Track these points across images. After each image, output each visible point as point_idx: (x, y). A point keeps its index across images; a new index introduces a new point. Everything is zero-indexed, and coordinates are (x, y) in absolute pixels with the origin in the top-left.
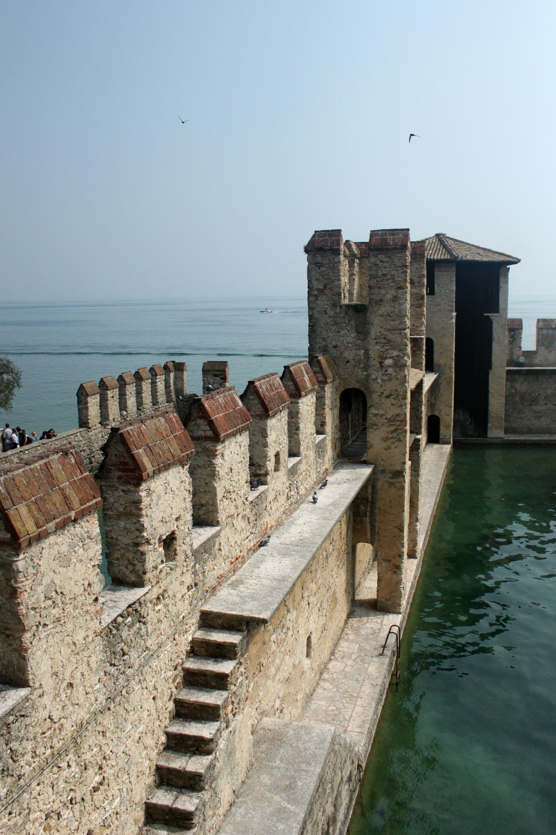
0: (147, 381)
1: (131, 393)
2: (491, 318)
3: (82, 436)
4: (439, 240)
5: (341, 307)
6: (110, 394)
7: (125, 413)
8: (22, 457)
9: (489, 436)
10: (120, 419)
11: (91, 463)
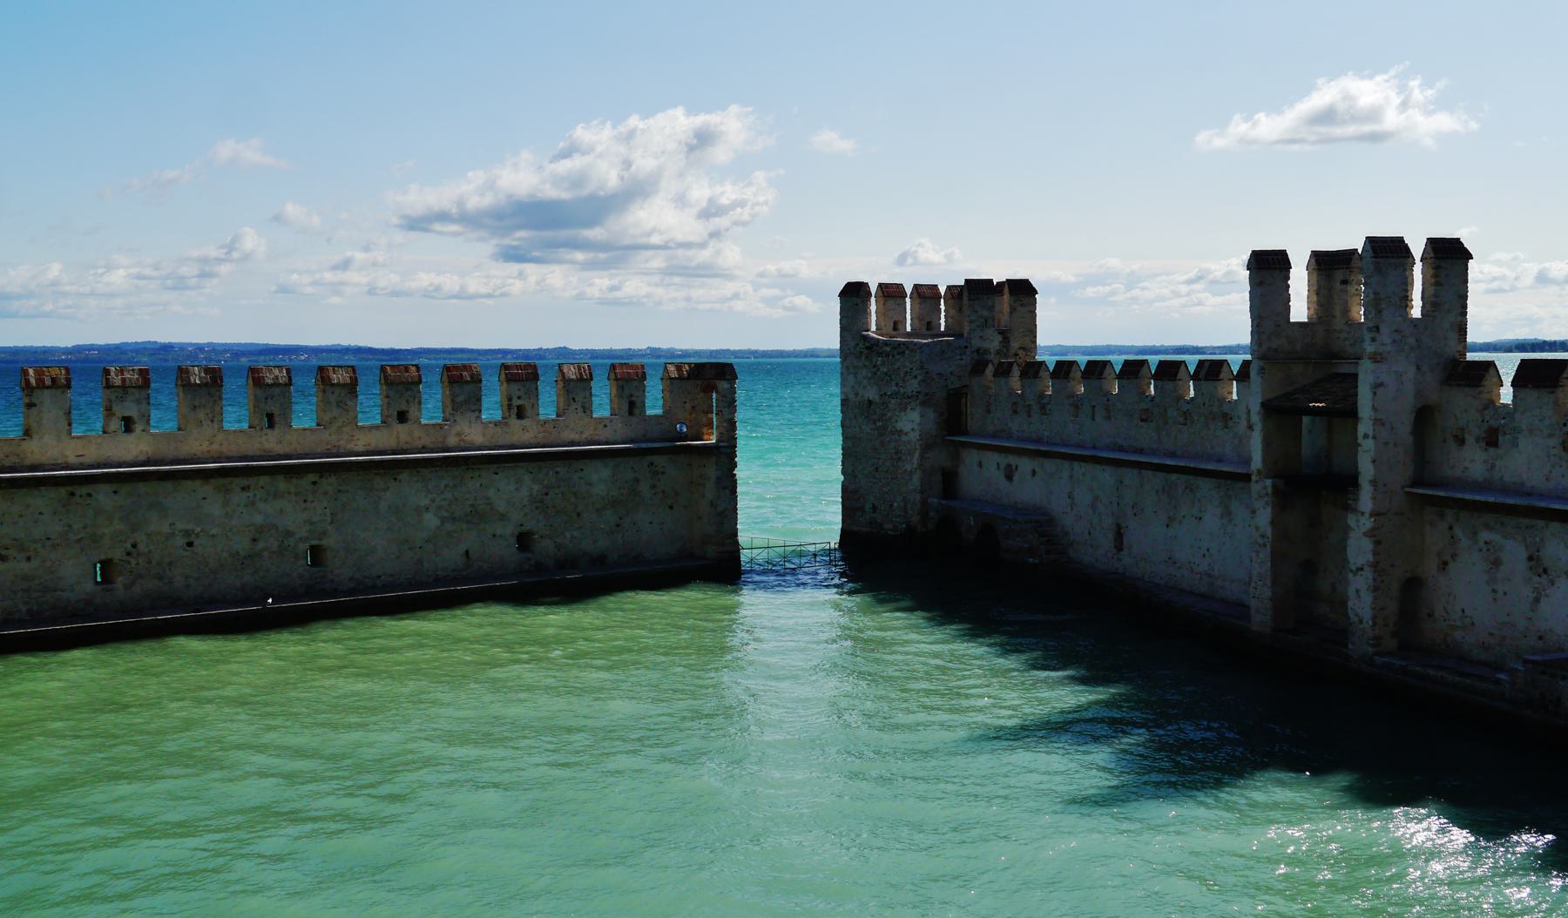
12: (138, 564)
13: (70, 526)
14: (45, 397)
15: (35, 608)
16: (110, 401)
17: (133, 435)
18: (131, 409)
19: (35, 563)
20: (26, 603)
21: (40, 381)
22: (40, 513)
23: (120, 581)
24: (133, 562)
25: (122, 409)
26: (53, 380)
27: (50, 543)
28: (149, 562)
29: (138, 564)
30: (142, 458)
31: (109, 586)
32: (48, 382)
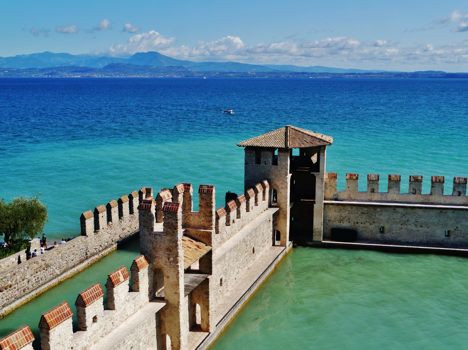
0: (126, 203)
1: (115, 212)
2: (315, 175)
3: (82, 241)
4: (286, 131)
5: (152, 234)
6: (100, 215)
7: (111, 223)
8: (44, 259)
9: (314, 240)
10: (107, 227)
11: (87, 254)
12: (458, 233)
13: (440, 220)
14: (437, 185)
15: (428, 240)
16: (455, 187)
17: (461, 196)
18: (460, 189)
19: (429, 229)
20: (426, 239)
21: (436, 180)
22: (432, 216)
23: (452, 237)
24: (456, 232)
25: (457, 189)
26: (439, 180)
27: (434, 224)
28: (461, 232)
29: (458, 233)
30: (462, 203)
31: (449, 238)
32: (438, 181)
